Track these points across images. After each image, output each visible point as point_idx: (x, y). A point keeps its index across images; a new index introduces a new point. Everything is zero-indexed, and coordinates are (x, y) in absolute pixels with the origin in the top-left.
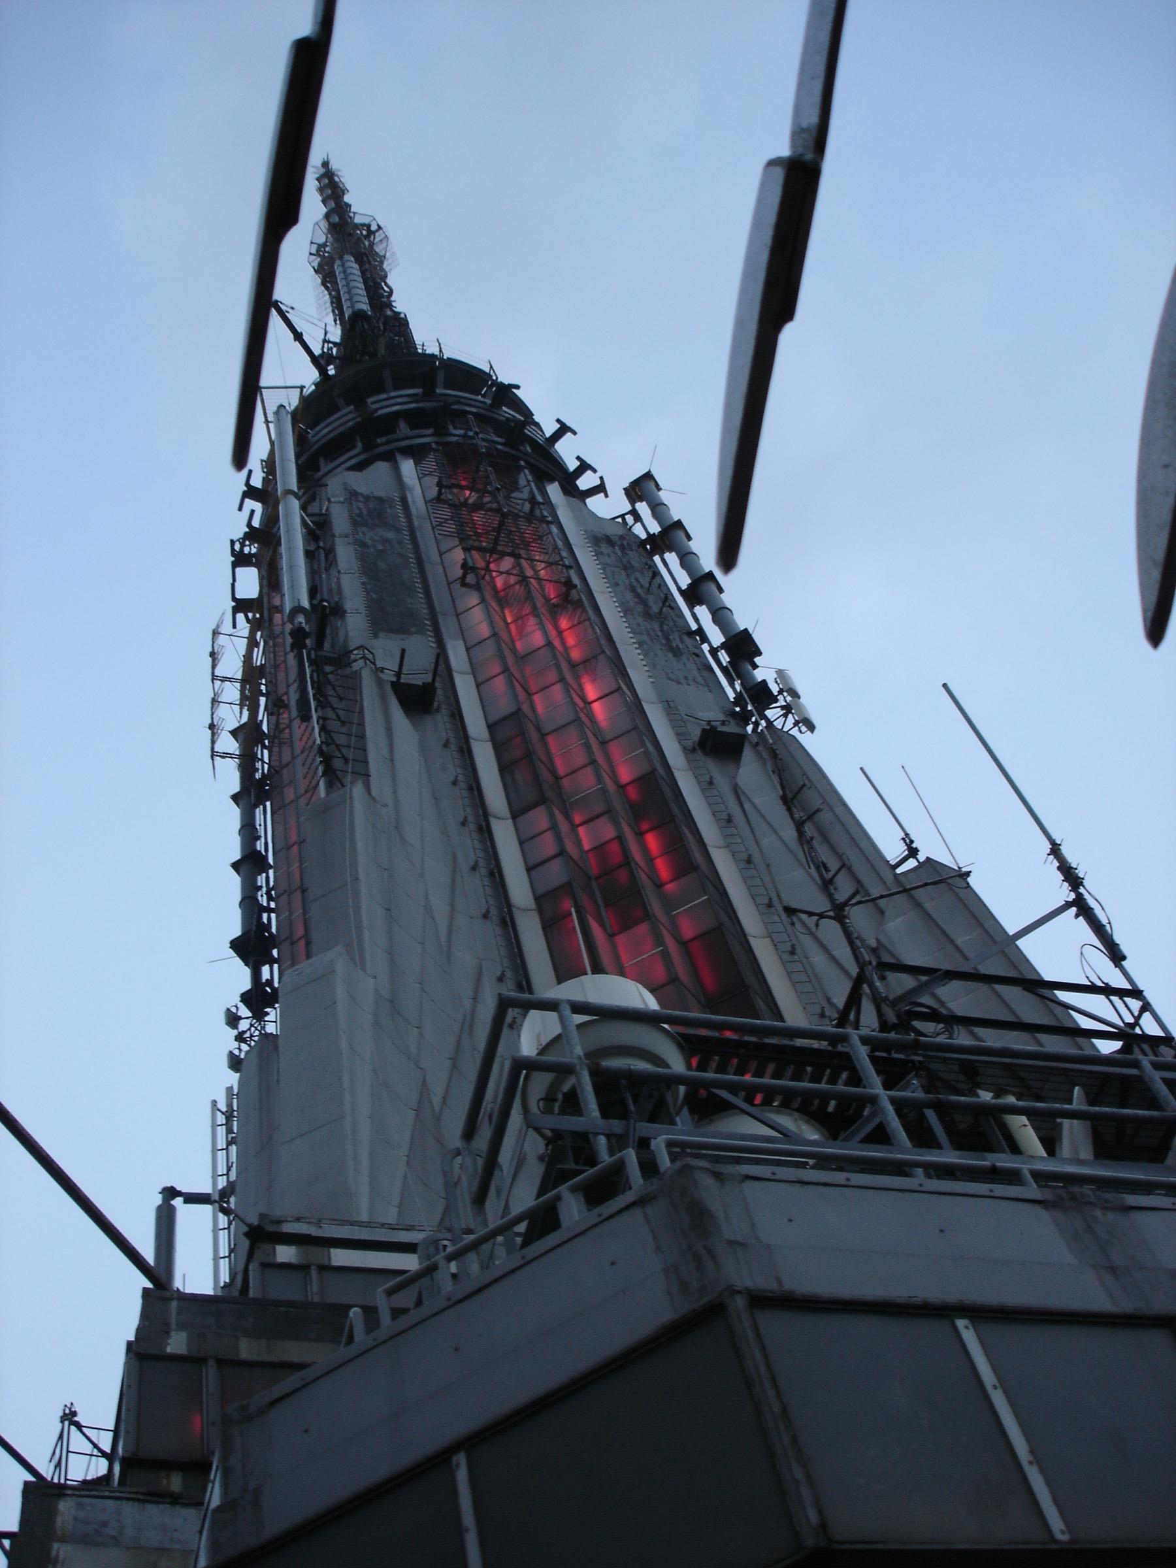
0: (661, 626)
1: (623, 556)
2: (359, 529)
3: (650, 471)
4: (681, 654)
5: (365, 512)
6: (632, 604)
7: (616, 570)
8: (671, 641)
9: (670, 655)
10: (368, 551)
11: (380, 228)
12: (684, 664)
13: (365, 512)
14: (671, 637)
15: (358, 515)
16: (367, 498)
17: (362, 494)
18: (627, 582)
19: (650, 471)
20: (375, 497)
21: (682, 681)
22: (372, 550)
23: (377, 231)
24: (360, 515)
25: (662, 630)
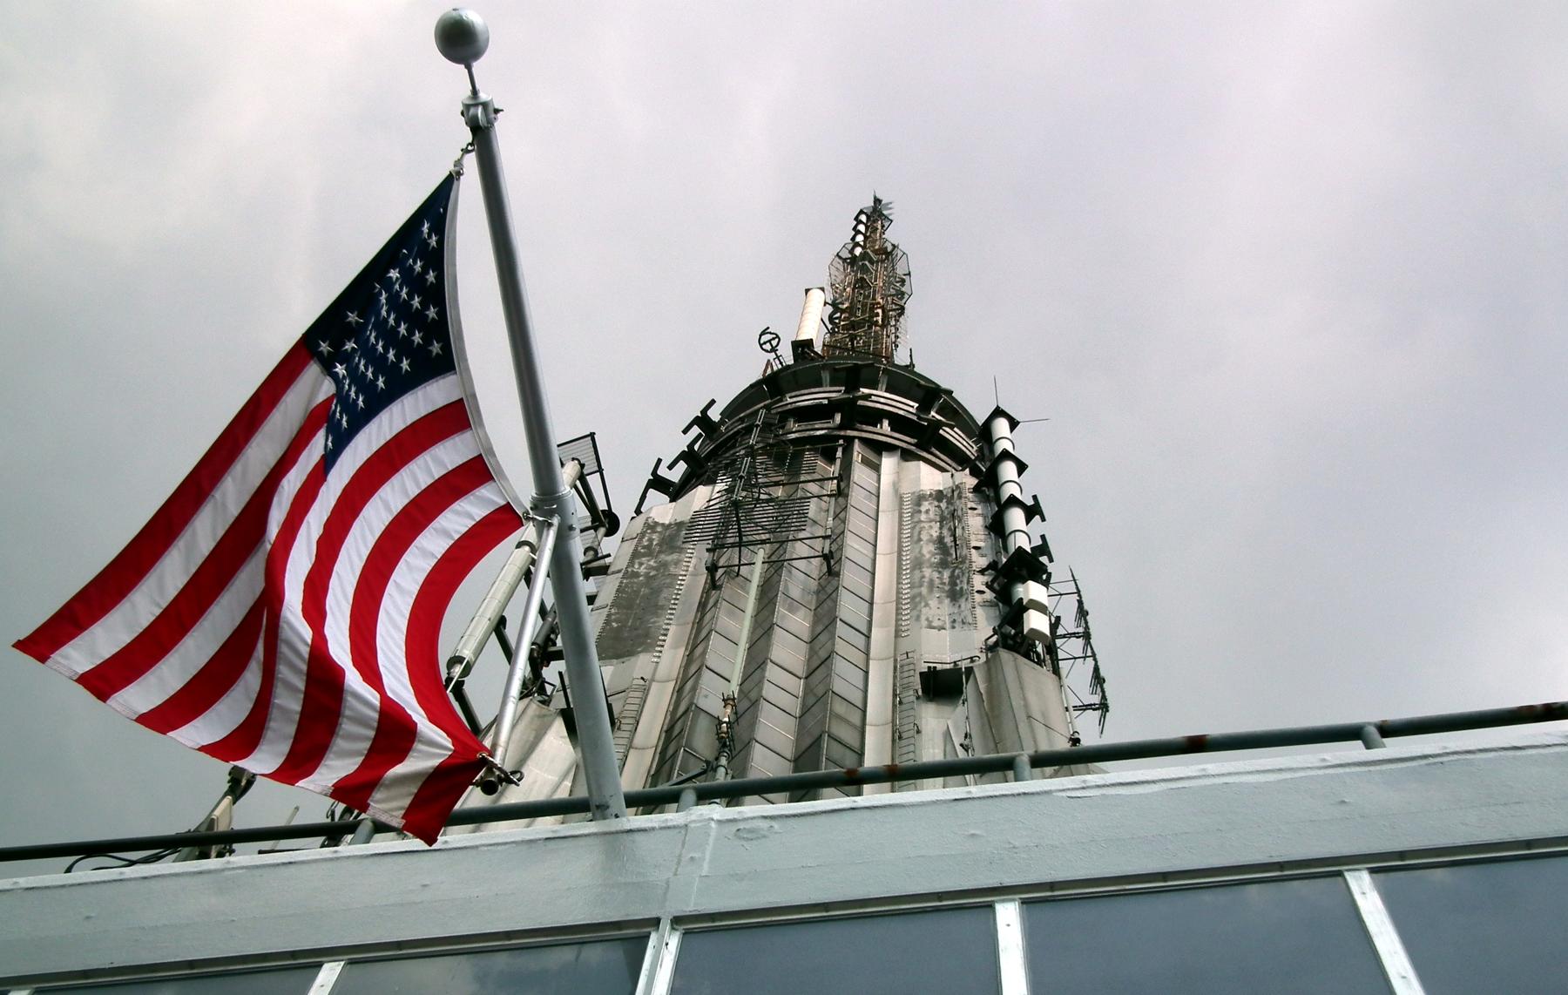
0: (954, 571)
1: (947, 508)
2: (637, 561)
3: (998, 407)
4: (962, 595)
5: (655, 543)
6: (928, 556)
7: (926, 525)
8: (957, 585)
9: (947, 601)
10: (636, 580)
11: (894, 246)
12: (960, 606)
13: (655, 543)
14: (958, 581)
15: (644, 547)
16: (666, 527)
17: (663, 525)
18: (935, 535)
19: (998, 407)
20: (676, 524)
21: (948, 626)
22: (641, 578)
23: (893, 250)
24: (648, 547)
25: (952, 577)
